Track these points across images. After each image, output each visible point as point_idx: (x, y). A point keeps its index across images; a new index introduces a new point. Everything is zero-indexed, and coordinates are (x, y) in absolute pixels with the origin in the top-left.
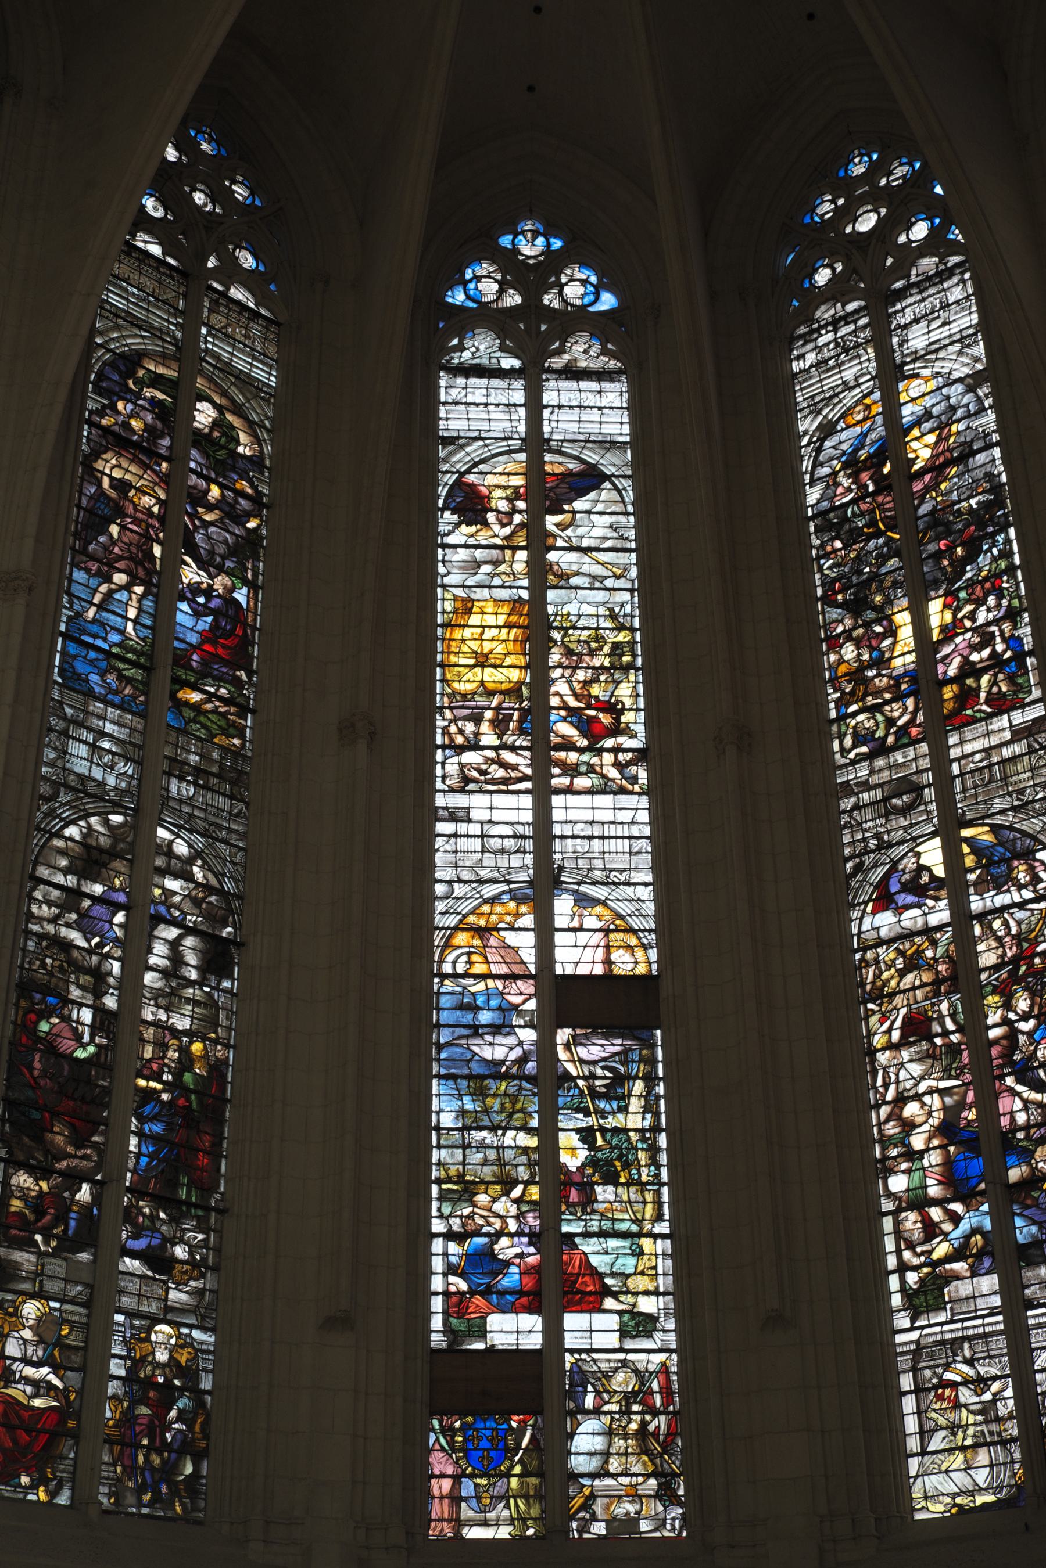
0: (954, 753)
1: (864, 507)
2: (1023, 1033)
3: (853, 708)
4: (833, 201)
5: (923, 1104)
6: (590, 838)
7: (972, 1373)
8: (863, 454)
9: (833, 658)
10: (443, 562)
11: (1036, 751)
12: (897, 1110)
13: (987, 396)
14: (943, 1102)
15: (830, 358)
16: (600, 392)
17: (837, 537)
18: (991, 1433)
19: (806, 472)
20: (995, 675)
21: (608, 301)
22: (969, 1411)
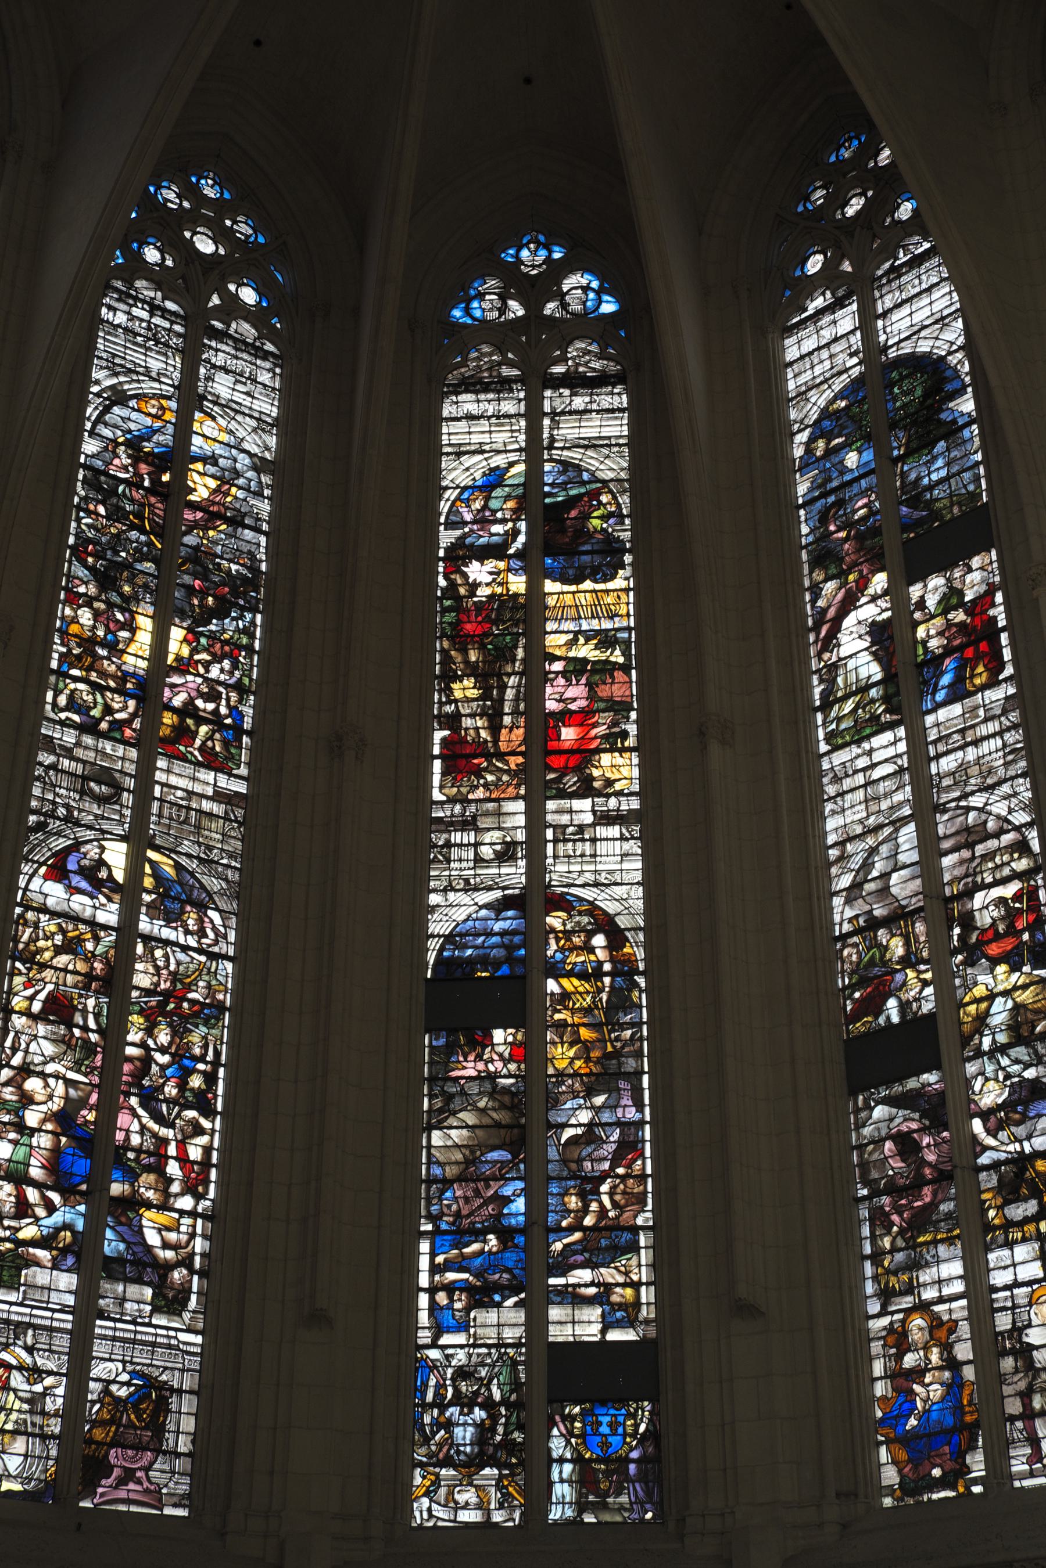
0: (159, 776)
1: (138, 495)
2: (157, 1064)
3: (75, 672)
4: (178, 196)
5: (47, 1085)
7: (29, 1360)
8: (147, 447)
11: (231, 821)
12: (18, 1078)
13: (268, 486)
14: (67, 1092)
15: (141, 335)
17: (103, 502)
18: (34, 1424)
19: (89, 419)
20: (214, 732)
22: (16, 1396)
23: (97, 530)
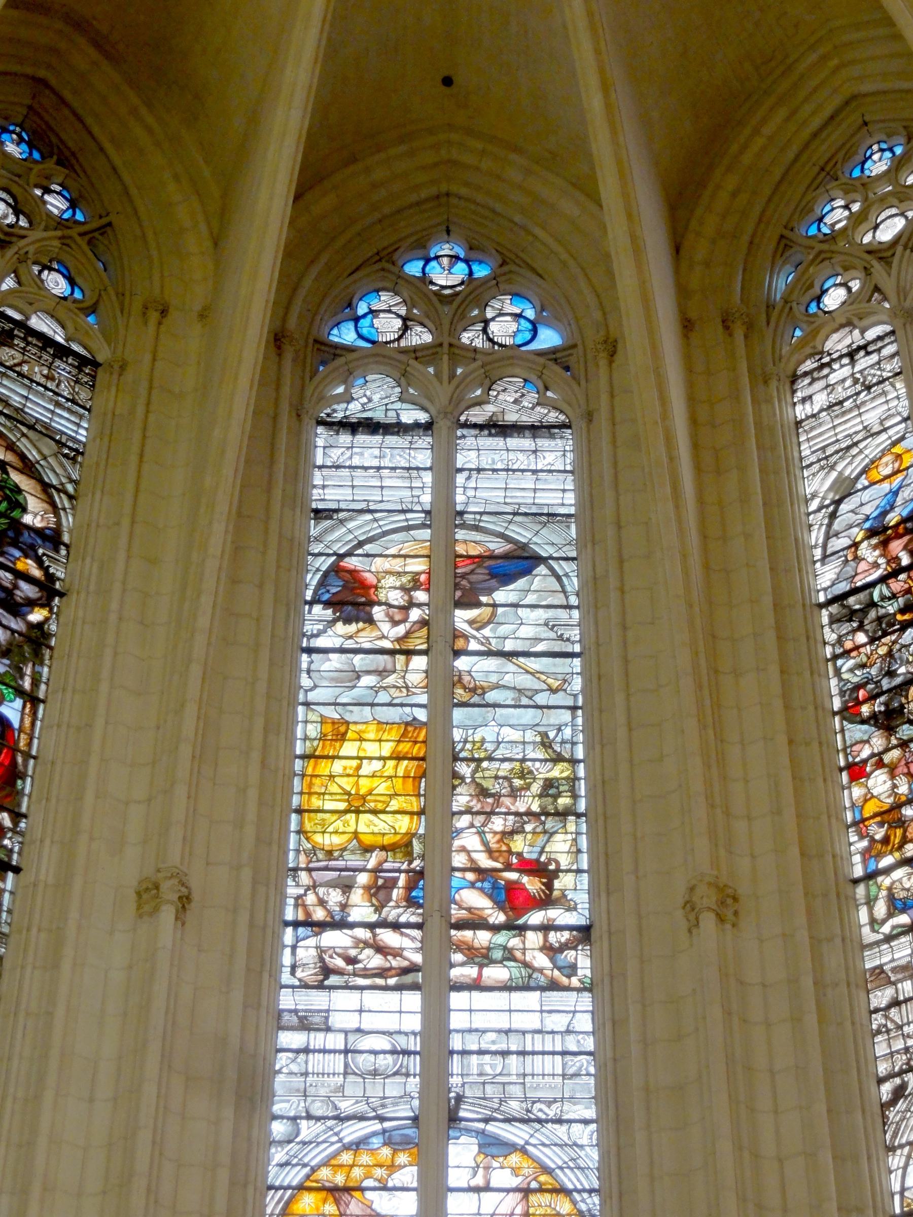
4: (846, 207)
6: (505, 1054)
8: (893, 518)
9: (857, 792)
10: (309, 672)
16: (535, 452)
17: (861, 628)
19: (815, 546)
21: (549, 338)
23: (863, 666)
